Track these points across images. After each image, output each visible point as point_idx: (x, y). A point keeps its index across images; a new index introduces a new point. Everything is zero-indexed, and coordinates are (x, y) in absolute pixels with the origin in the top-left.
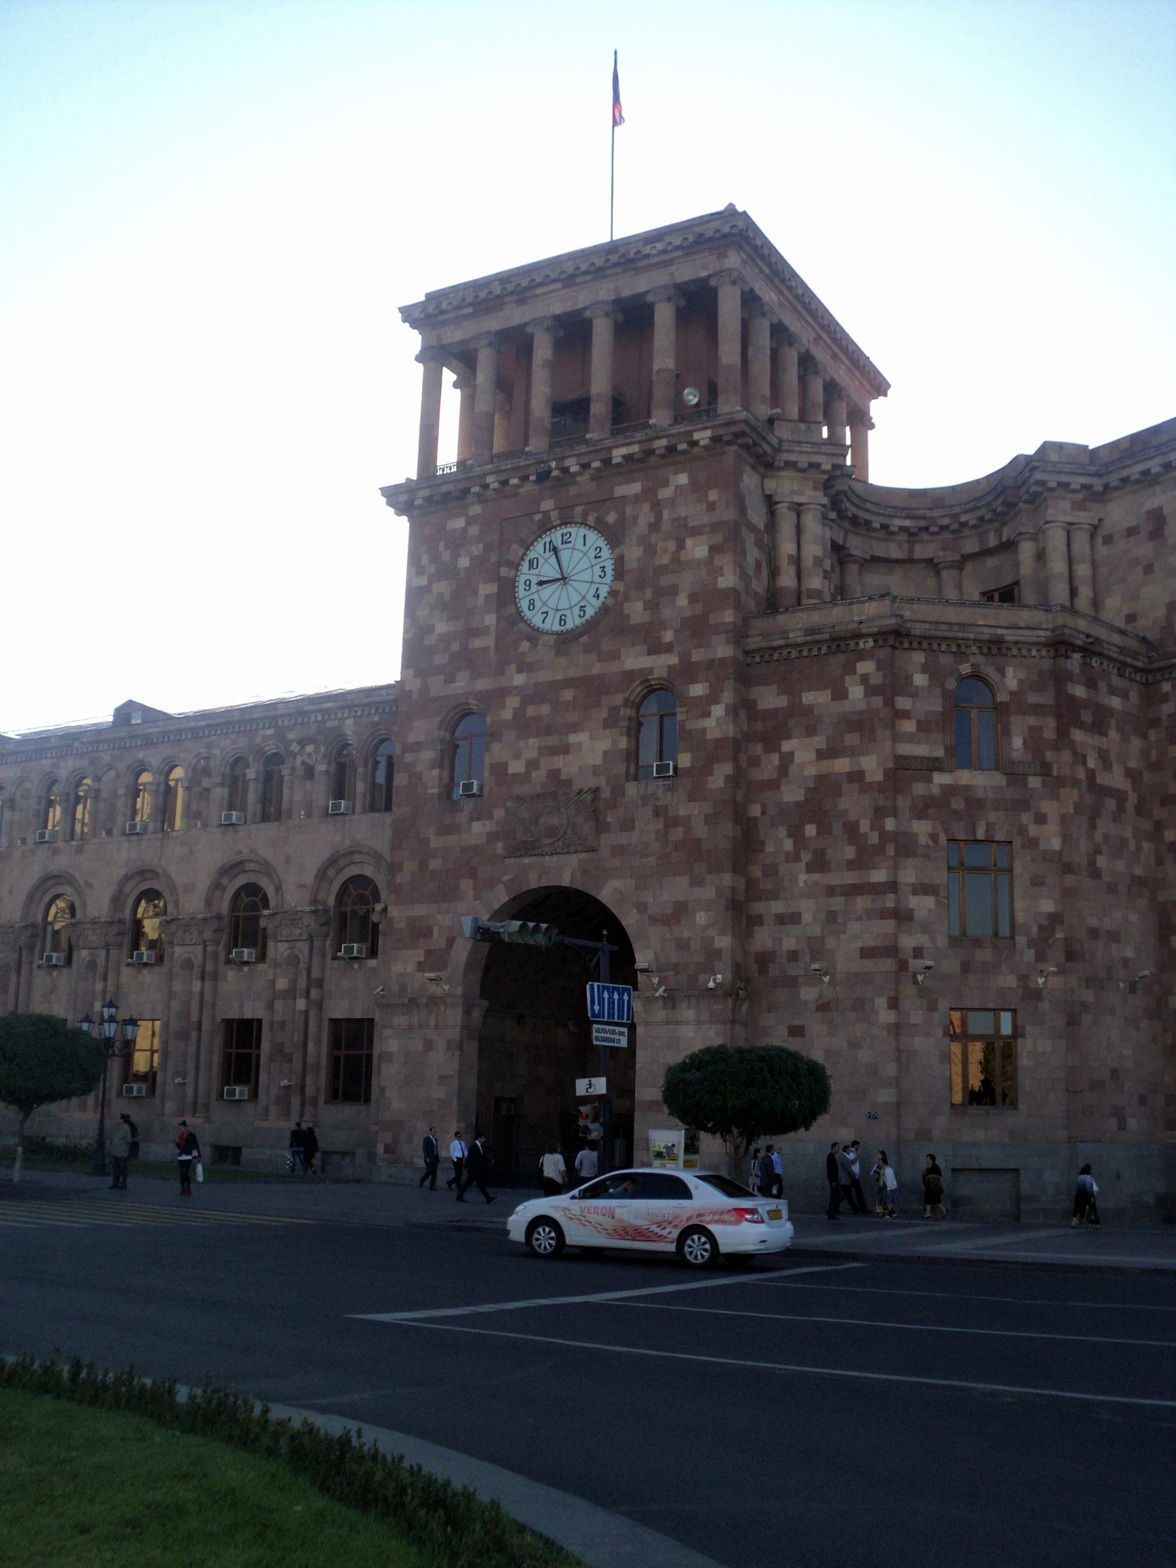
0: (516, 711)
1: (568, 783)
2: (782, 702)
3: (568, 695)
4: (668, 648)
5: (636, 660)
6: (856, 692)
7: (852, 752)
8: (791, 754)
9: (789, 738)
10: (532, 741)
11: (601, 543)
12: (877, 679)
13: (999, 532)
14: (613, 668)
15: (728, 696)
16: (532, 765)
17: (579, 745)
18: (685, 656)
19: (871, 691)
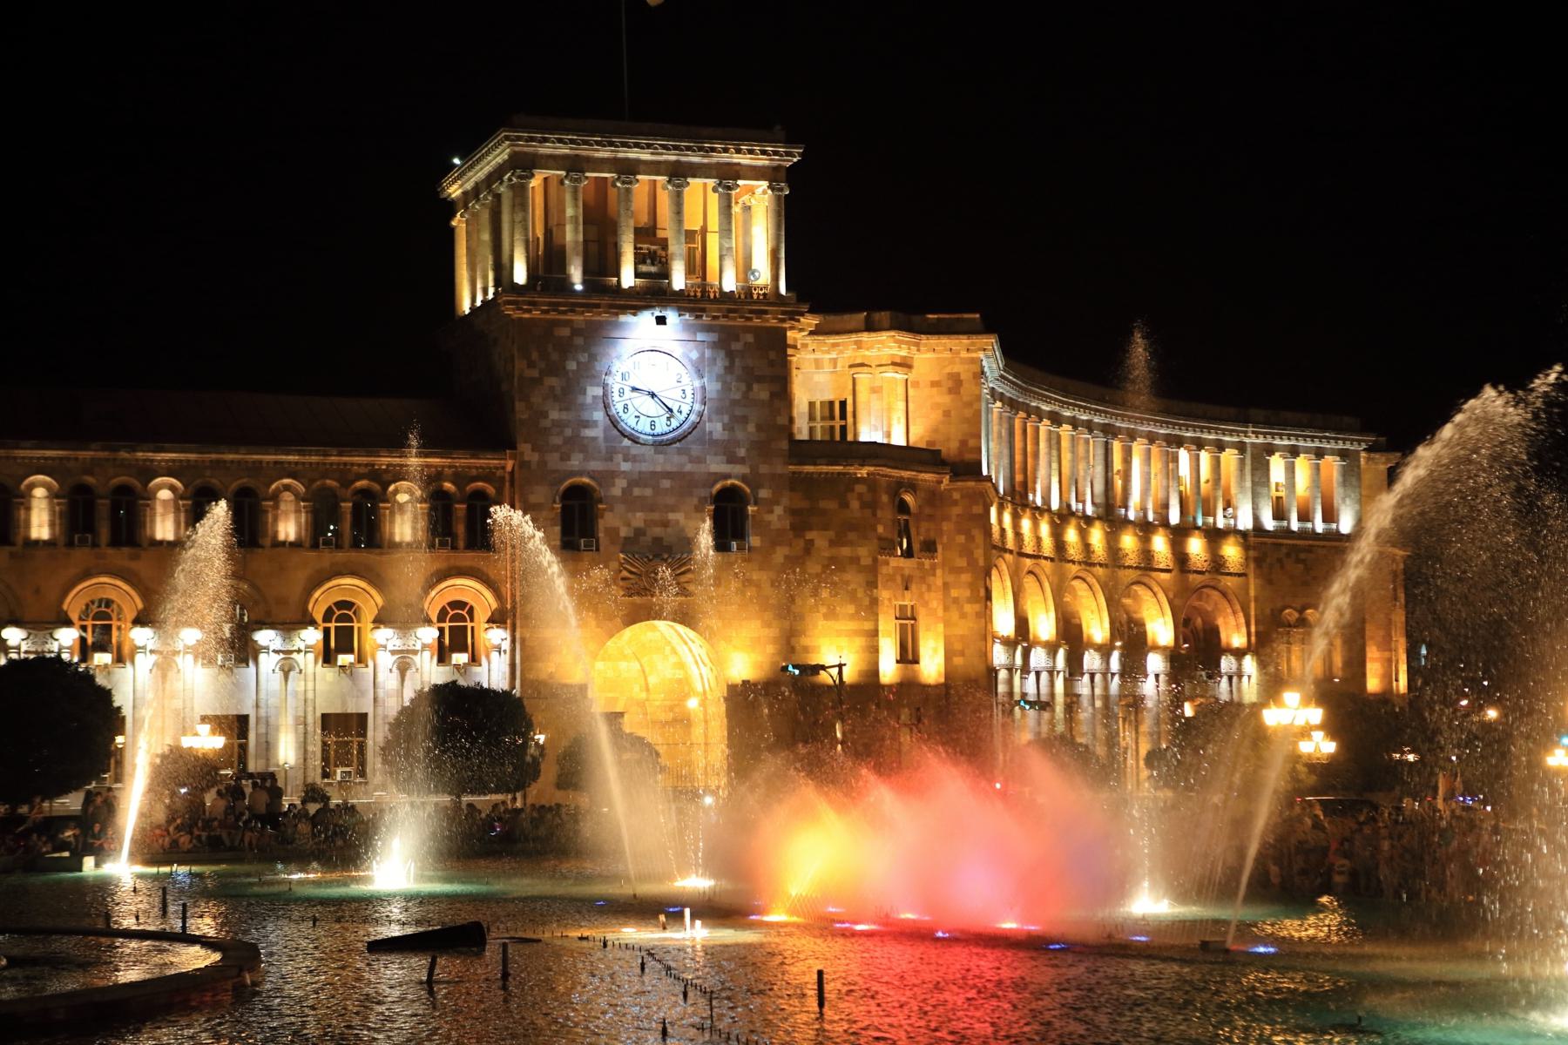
0: (624, 490)
1: (669, 549)
2: (804, 504)
3: (666, 484)
4: (742, 461)
5: (716, 465)
6: (855, 504)
7: (851, 544)
8: (811, 542)
9: (811, 529)
10: (639, 514)
11: (682, 370)
12: (868, 497)
13: (834, 362)
14: (701, 469)
15: (785, 501)
16: (639, 532)
17: (677, 522)
18: (754, 469)
19: (864, 505)
